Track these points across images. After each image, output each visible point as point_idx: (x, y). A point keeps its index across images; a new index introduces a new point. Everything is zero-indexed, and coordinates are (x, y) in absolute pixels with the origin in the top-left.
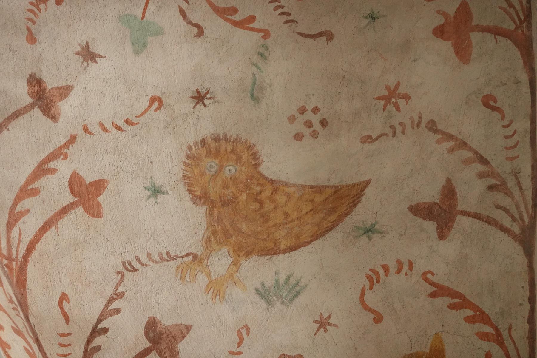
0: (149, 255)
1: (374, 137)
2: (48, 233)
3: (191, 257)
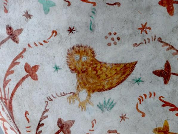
0: (56, 94)
1: (138, 44)
2: (19, 88)
3: (72, 94)
